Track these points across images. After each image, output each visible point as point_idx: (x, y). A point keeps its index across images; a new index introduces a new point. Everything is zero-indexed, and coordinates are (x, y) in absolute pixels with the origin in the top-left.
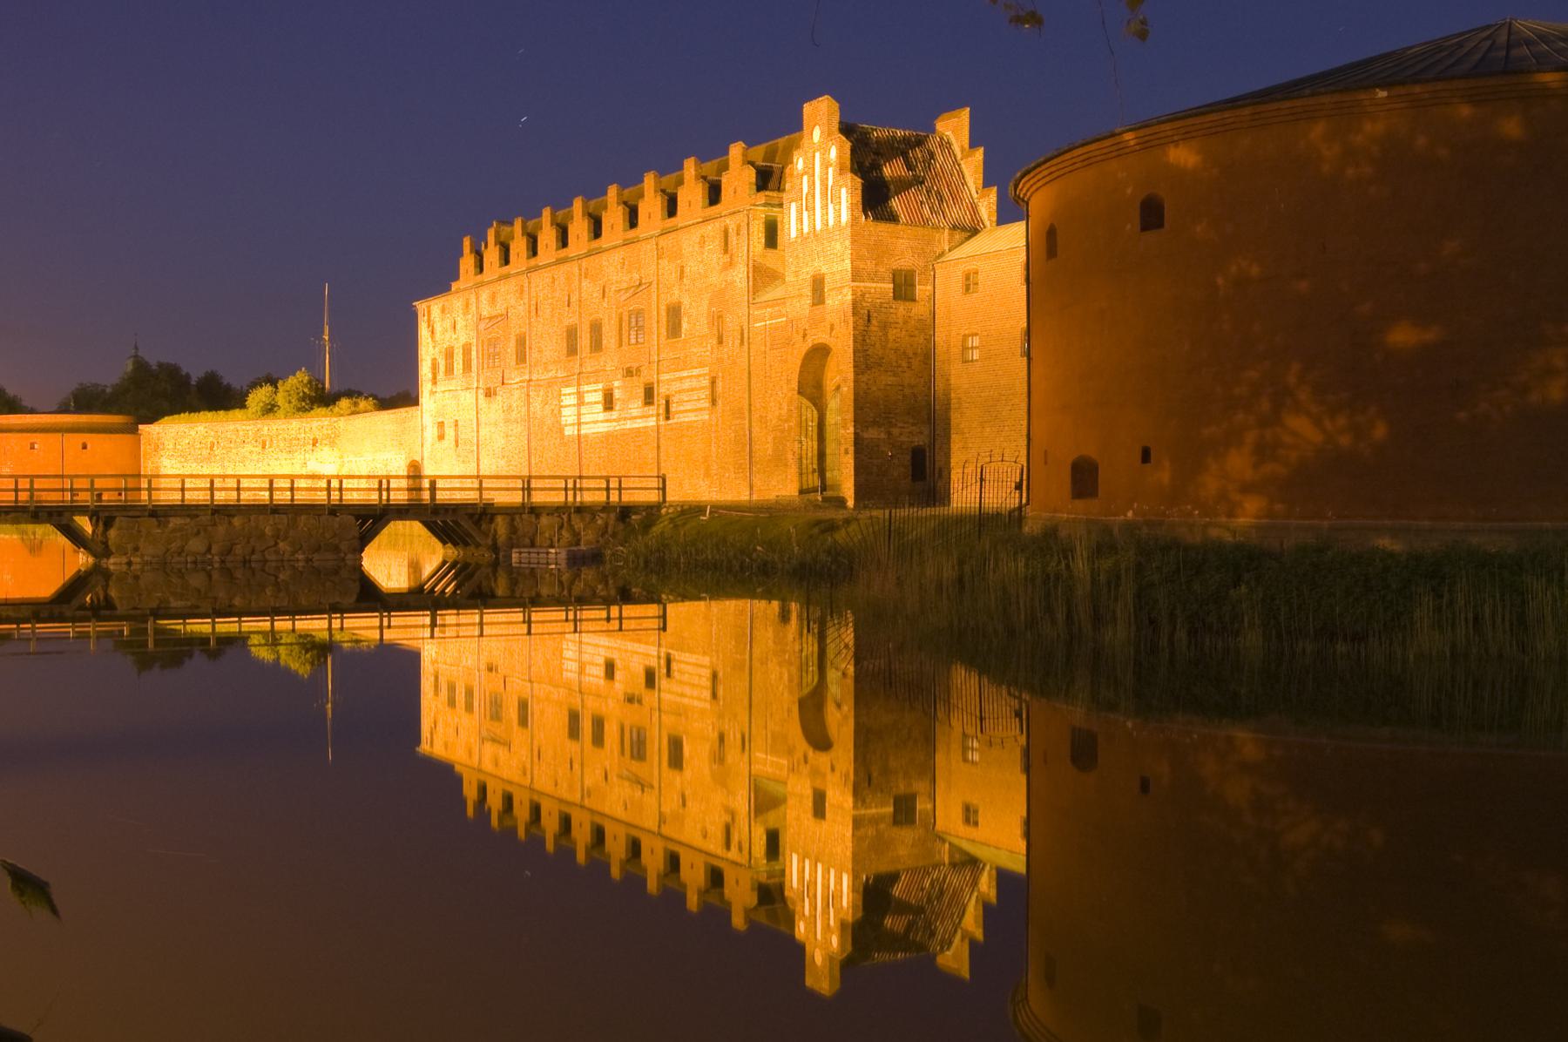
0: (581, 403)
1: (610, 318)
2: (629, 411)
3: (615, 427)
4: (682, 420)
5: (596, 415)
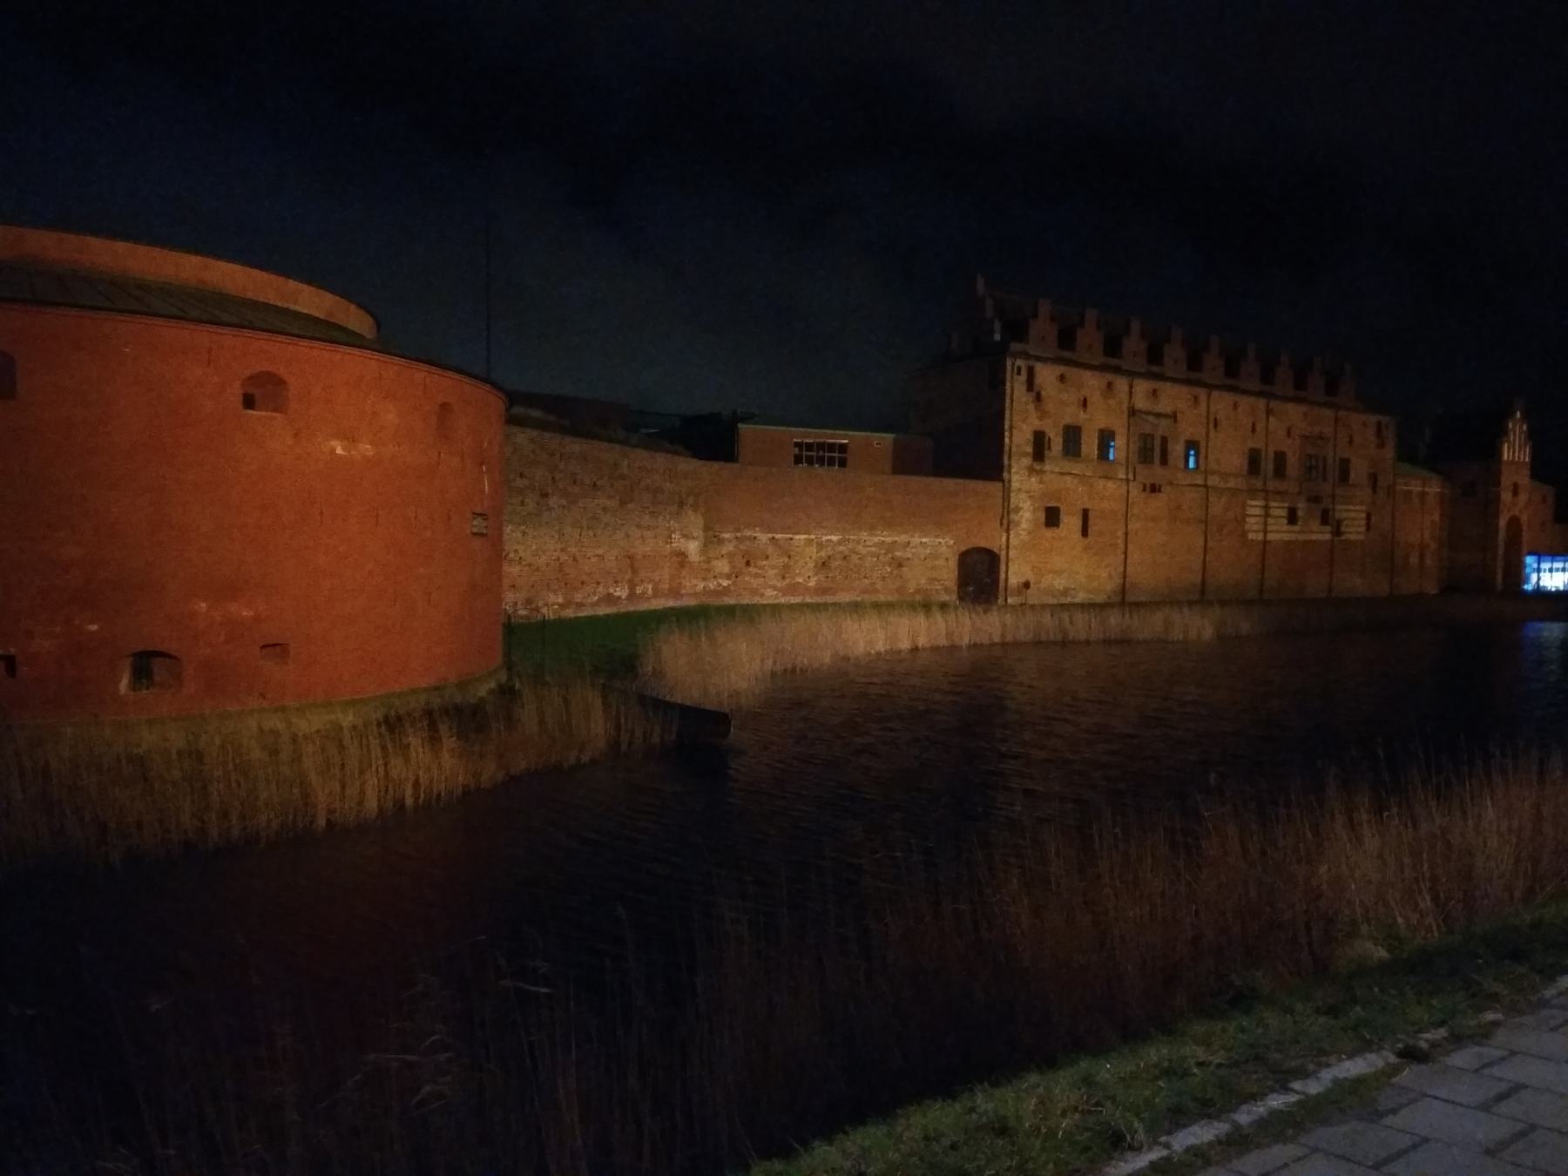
0: (1267, 515)
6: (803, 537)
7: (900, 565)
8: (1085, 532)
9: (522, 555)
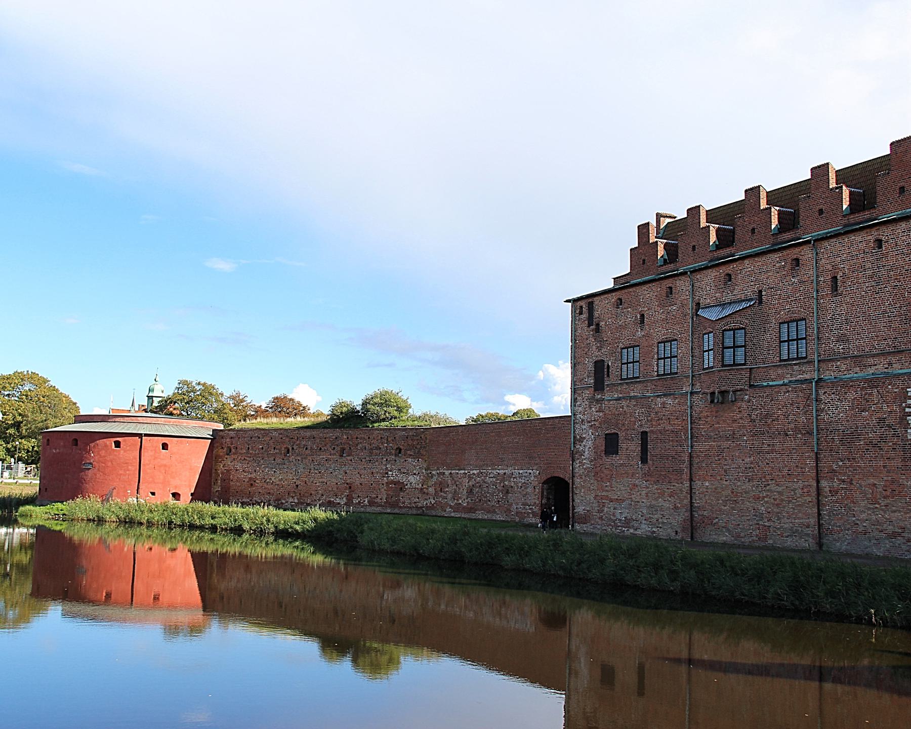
6: (464, 471)
7: (507, 492)
9: (274, 480)
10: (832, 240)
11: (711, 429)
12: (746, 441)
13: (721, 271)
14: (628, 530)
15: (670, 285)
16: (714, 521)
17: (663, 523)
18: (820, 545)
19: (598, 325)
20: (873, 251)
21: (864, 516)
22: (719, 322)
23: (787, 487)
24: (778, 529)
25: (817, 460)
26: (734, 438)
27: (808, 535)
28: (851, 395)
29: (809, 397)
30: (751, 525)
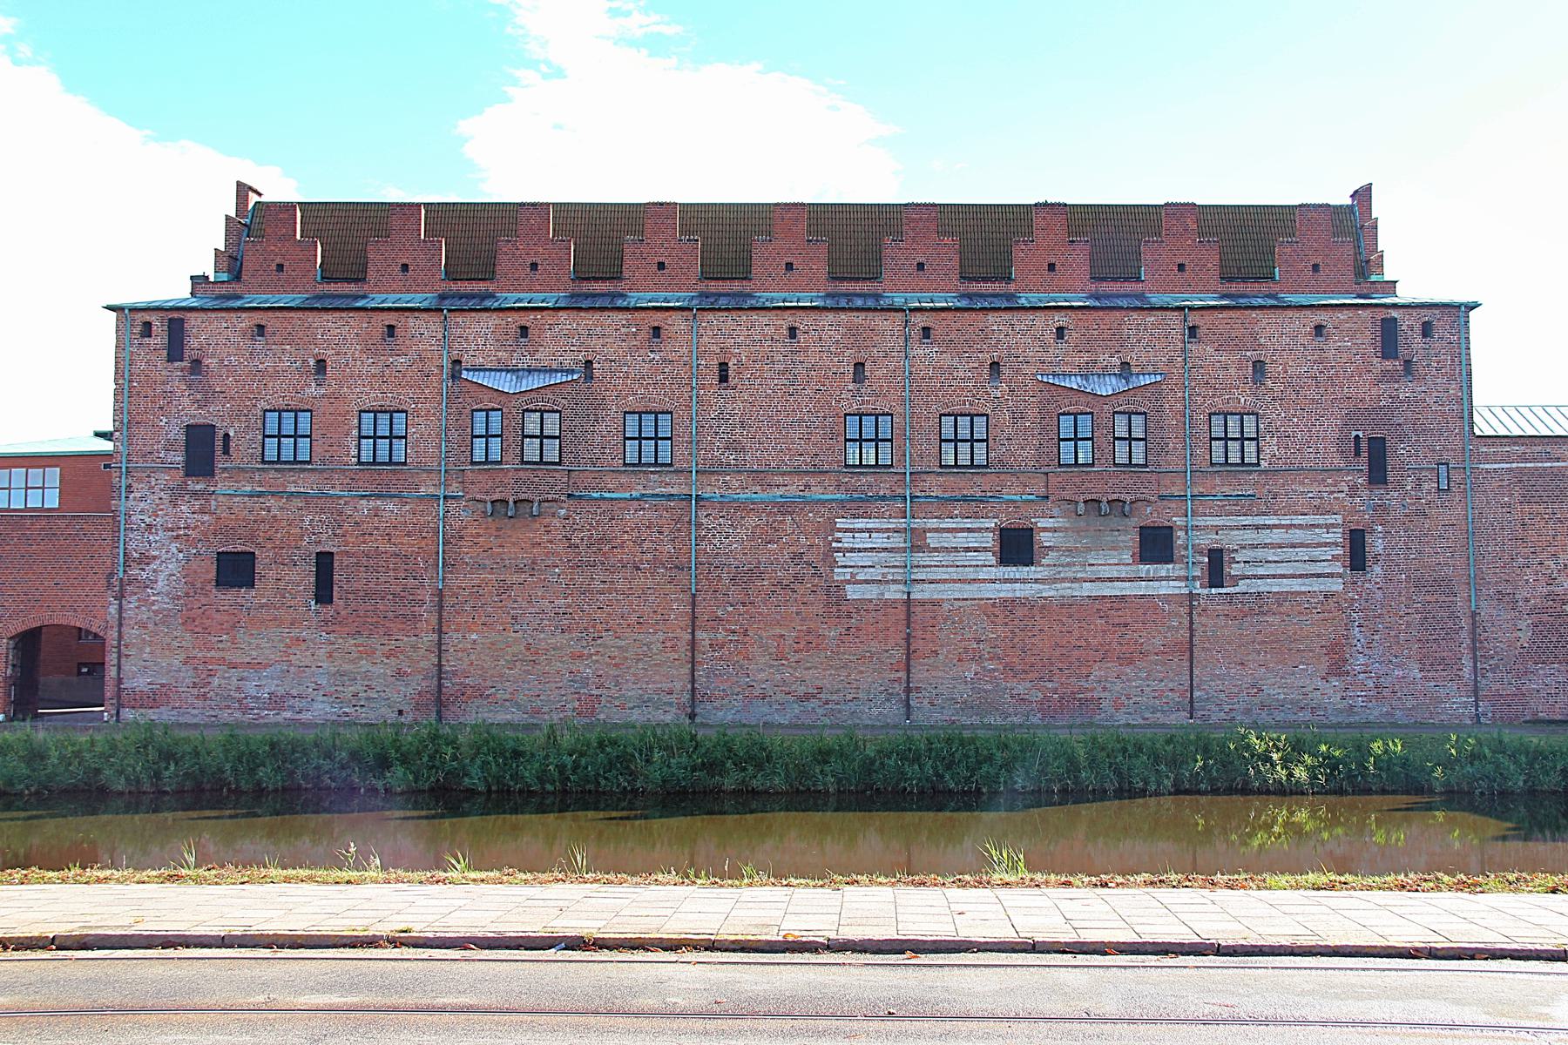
1: (1018, 415)
2: (1094, 568)
3: (1041, 591)
4: (1261, 589)
5: (972, 569)
8: (324, 592)
10: (721, 314)
11: (485, 554)
12: (559, 575)
13: (509, 320)
14: (278, 714)
15: (393, 323)
16: (487, 693)
17: (368, 699)
18: (692, 716)
19: (197, 363)
20: (786, 340)
21: (762, 675)
22: (517, 396)
23: (635, 640)
24: (617, 698)
25: (694, 605)
26: (533, 569)
27: (671, 704)
28: (752, 521)
29: (680, 518)
30: (564, 695)
